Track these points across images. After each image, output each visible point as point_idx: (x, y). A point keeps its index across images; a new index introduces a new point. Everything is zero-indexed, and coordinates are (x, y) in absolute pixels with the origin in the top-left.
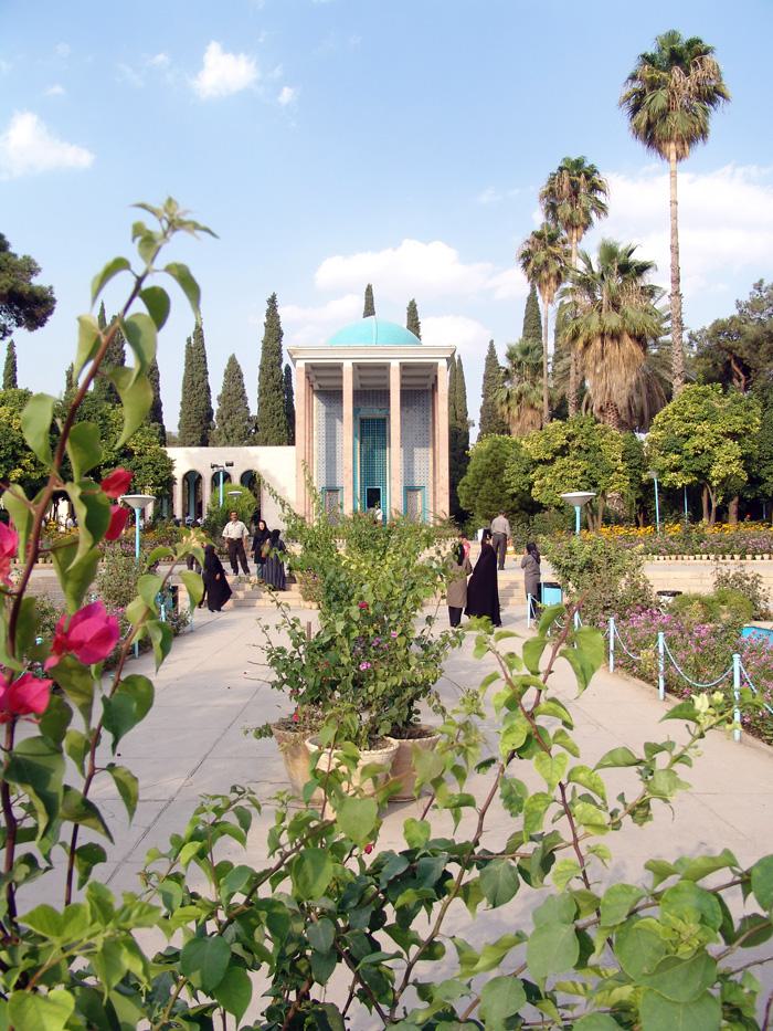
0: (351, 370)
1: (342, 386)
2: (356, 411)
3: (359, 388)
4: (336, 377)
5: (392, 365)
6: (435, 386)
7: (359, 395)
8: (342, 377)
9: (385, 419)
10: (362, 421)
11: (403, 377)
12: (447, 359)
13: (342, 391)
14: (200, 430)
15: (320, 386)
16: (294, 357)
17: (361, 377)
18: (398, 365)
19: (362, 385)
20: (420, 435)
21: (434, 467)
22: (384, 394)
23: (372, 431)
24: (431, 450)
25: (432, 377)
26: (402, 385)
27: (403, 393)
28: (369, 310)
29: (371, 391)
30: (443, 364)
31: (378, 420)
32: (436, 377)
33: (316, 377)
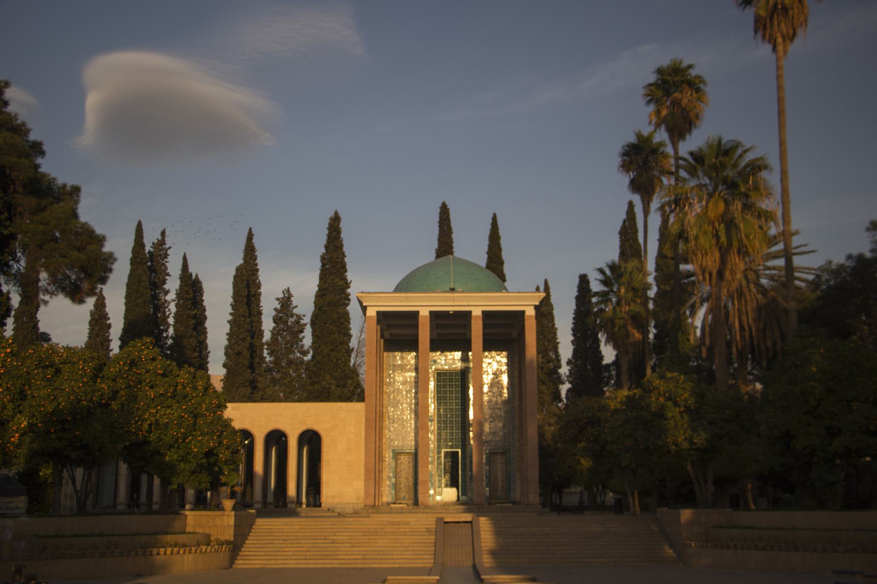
0: (428, 320)
1: (417, 335)
3: (435, 337)
5: (473, 314)
8: (416, 326)
11: (485, 326)
14: (252, 377)
15: (391, 335)
16: (364, 304)
19: (438, 335)
26: (484, 335)
28: (445, 247)
30: (530, 312)
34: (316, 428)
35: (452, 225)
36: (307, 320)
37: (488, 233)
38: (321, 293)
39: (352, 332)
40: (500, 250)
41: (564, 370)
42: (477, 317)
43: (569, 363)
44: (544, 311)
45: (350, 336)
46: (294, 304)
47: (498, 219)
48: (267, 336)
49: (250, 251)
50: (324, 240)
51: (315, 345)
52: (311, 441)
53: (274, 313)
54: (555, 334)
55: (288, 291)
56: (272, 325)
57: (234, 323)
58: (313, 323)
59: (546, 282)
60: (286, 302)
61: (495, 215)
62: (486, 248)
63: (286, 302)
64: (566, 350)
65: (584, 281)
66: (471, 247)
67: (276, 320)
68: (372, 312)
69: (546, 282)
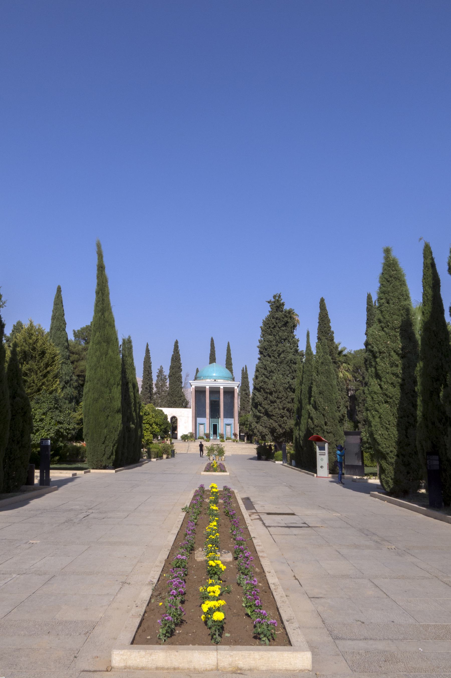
35: (215, 346)
36: (167, 377)
37: (226, 349)
38: (172, 368)
39: (183, 381)
40: (230, 354)
45: (181, 382)
46: (164, 371)
47: (230, 344)
48: (154, 382)
50: (172, 350)
51: (170, 384)
53: (157, 374)
54: (248, 384)
55: (161, 367)
56: (156, 378)
57: (144, 377)
58: (169, 376)
59: (246, 366)
60: (161, 372)
62: (226, 354)
63: (161, 372)
66: (221, 355)
67: (158, 376)
68: (193, 387)
69: (246, 366)
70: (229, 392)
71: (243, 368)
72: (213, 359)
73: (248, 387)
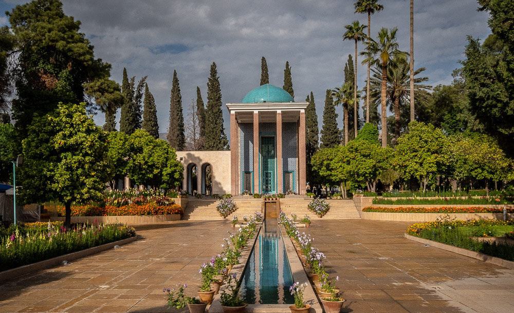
2: (260, 133)
4: (250, 117)
6: (299, 121)
7: (262, 125)
9: (274, 137)
10: (262, 138)
11: (282, 117)
12: (305, 109)
13: (253, 124)
16: (230, 109)
17: (262, 117)
18: (280, 112)
20: (291, 151)
21: (297, 165)
22: (273, 125)
23: (267, 142)
24: (297, 159)
25: (298, 117)
27: (283, 124)
29: (267, 124)
30: (303, 111)
31: (271, 137)
32: (299, 117)
33: (240, 117)
34: (209, 162)
41: (320, 136)
42: (279, 114)
43: (322, 132)
44: (311, 110)
49: (176, 81)
52: (206, 167)
59: (312, 93)
61: (287, 62)
64: (321, 126)
65: (328, 92)
68: (233, 112)
69: (312, 93)
70: (291, 125)
71: (308, 97)
72: (265, 80)
73: (315, 123)
